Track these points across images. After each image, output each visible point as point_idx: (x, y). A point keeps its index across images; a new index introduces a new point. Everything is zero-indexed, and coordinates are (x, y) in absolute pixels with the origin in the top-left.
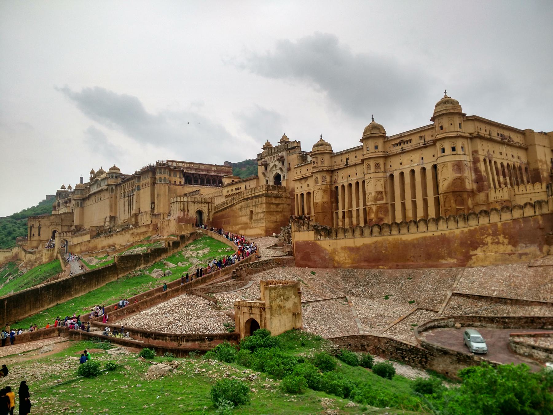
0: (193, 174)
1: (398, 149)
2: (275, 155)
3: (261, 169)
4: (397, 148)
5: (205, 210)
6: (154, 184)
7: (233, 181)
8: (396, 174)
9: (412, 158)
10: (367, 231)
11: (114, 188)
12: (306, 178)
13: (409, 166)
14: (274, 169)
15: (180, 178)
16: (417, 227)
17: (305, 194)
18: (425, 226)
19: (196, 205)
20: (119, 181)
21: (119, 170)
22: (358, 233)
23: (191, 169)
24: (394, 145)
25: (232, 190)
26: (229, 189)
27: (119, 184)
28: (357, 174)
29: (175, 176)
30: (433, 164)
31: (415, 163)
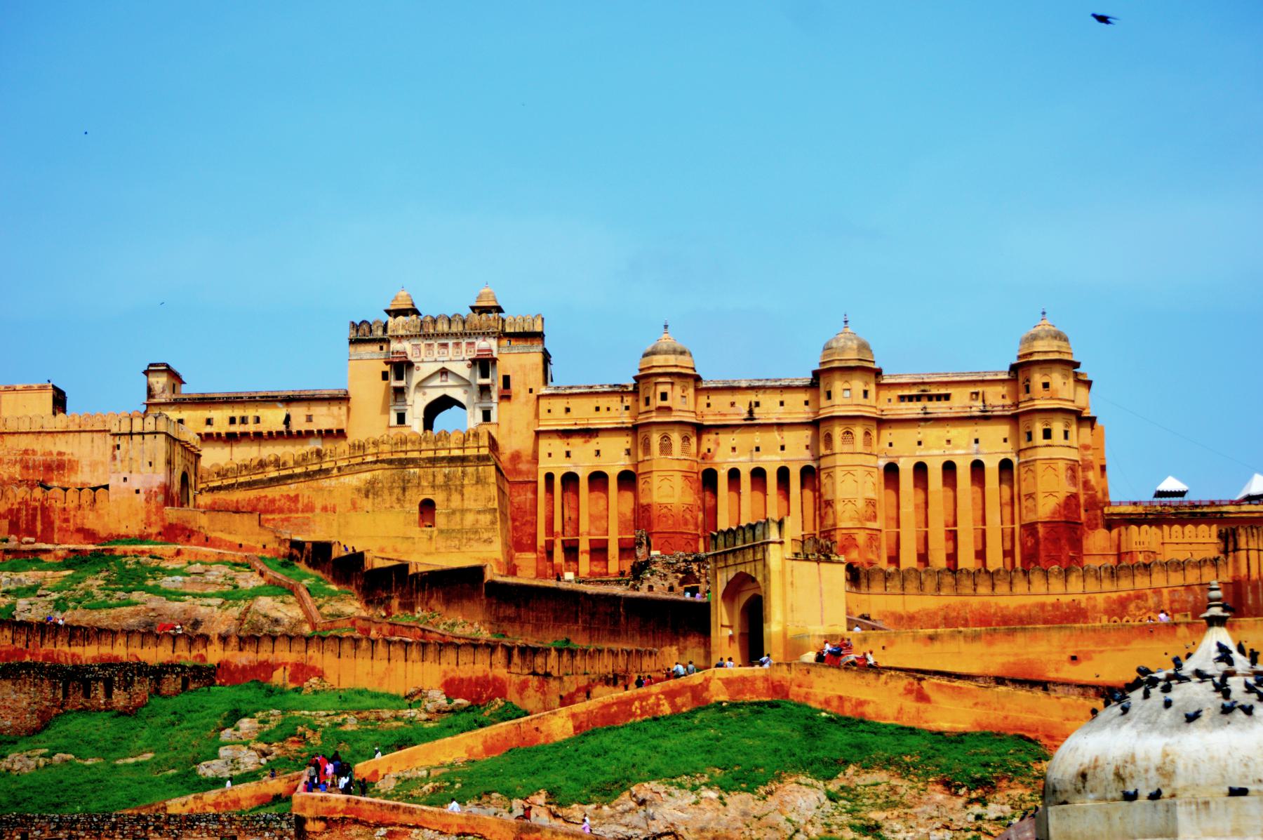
1: (913, 410)
2: (451, 342)
4: (911, 405)
9: (949, 436)
10: (911, 586)
12: (589, 433)
13: (941, 452)
16: (1029, 582)
17: (583, 475)
18: (1043, 581)
28: (783, 448)
30: (1003, 457)
31: (957, 447)
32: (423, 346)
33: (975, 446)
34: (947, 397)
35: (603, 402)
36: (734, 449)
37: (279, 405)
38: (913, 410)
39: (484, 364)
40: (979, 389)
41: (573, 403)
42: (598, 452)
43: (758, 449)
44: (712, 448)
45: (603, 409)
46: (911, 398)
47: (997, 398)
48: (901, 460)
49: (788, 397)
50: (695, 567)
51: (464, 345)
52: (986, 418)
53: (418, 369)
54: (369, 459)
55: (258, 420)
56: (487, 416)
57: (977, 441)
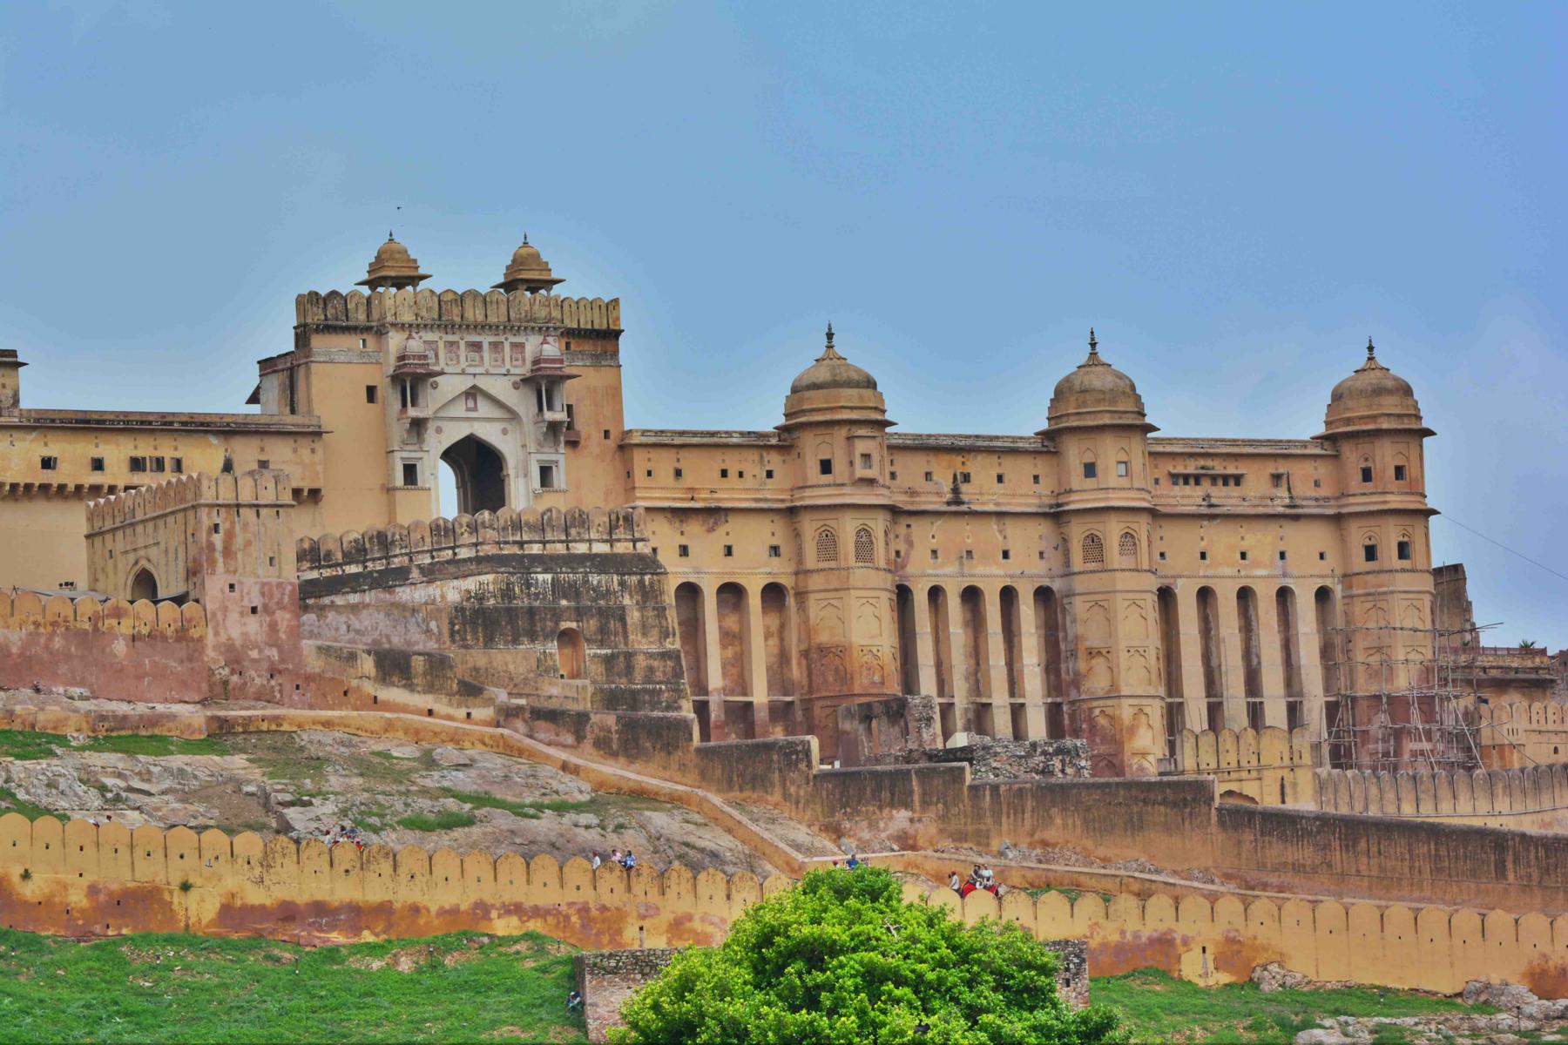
1: (1189, 498)
2: (486, 339)
4: (1188, 490)
9: (1244, 546)
12: (714, 514)
14: (459, 410)
24: (1175, 478)
28: (1006, 555)
30: (1320, 583)
31: (1258, 565)
32: (441, 344)
33: (1280, 563)
34: (1238, 480)
35: (733, 462)
36: (934, 552)
37: (214, 440)
39: (542, 384)
40: (1282, 467)
41: (688, 461)
42: (729, 551)
43: (969, 553)
44: (903, 548)
45: (733, 473)
46: (1186, 479)
47: (1308, 482)
48: (1180, 582)
49: (1010, 466)
50: (1056, 763)
51: (507, 348)
52: (1293, 517)
53: (435, 386)
54: (464, 553)
55: (178, 465)
56: (546, 472)
57: (1282, 555)
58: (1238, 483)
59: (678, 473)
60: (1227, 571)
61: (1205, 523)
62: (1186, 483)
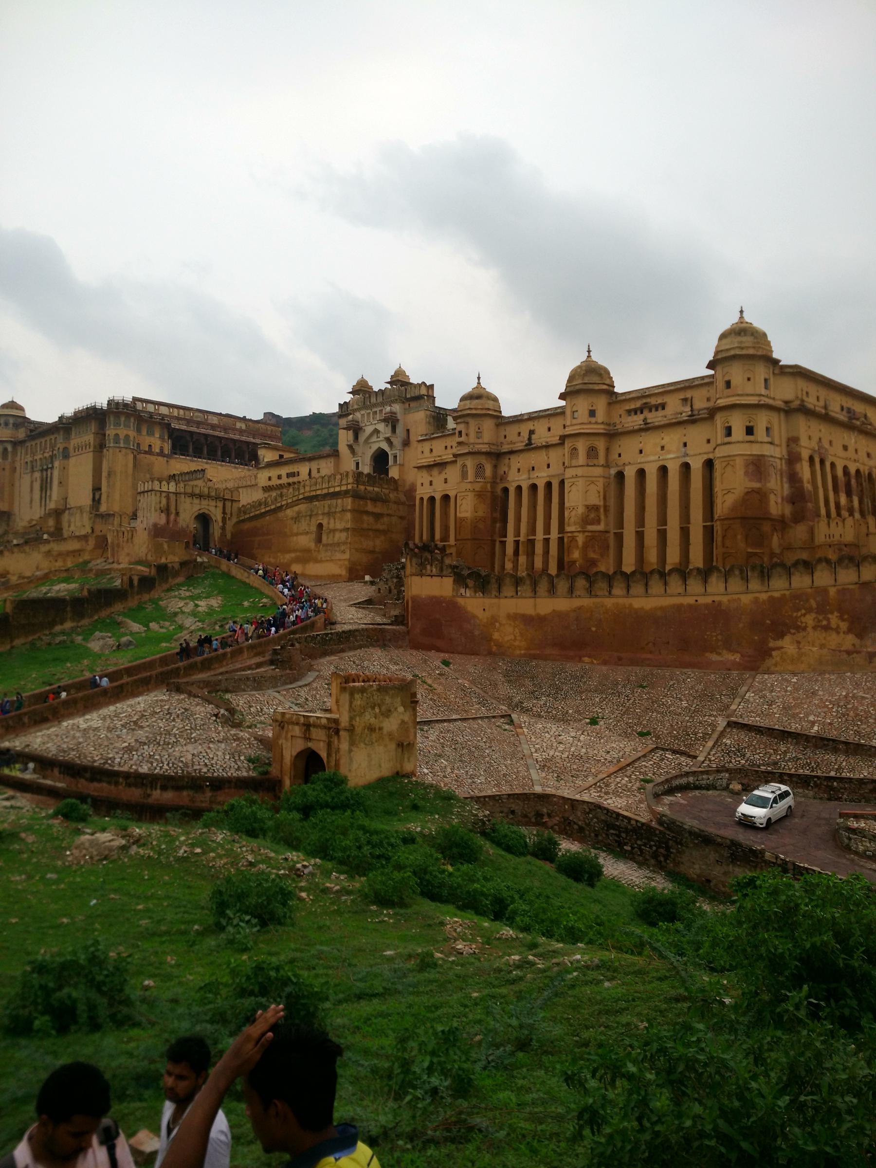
0: (192, 433)
2: (378, 409)
3: (344, 438)
4: (635, 418)
5: (216, 514)
6: (100, 447)
7: (281, 456)
8: (630, 473)
9: (663, 443)
10: (562, 586)
11: (10, 449)
12: (441, 465)
14: (374, 439)
15: (162, 438)
16: (666, 584)
17: (438, 497)
18: (680, 583)
19: (196, 501)
20: (21, 434)
21: (21, 409)
22: (543, 586)
23: (189, 422)
24: (629, 412)
25: (279, 477)
26: (274, 472)
27: (22, 442)
28: (548, 466)
29: (150, 433)
30: (706, 457)
31: (669, 452)
36: (519, 470)
38: (636, 421)
40: (688, 394)
43: (533, 468)
45: (449, 447)
46: (635, 411)
57: (685, 445)
58: (663, 408)
59: (431, 450)
60: (652, 458)
61: (643, 434)
62: (636, 413)
